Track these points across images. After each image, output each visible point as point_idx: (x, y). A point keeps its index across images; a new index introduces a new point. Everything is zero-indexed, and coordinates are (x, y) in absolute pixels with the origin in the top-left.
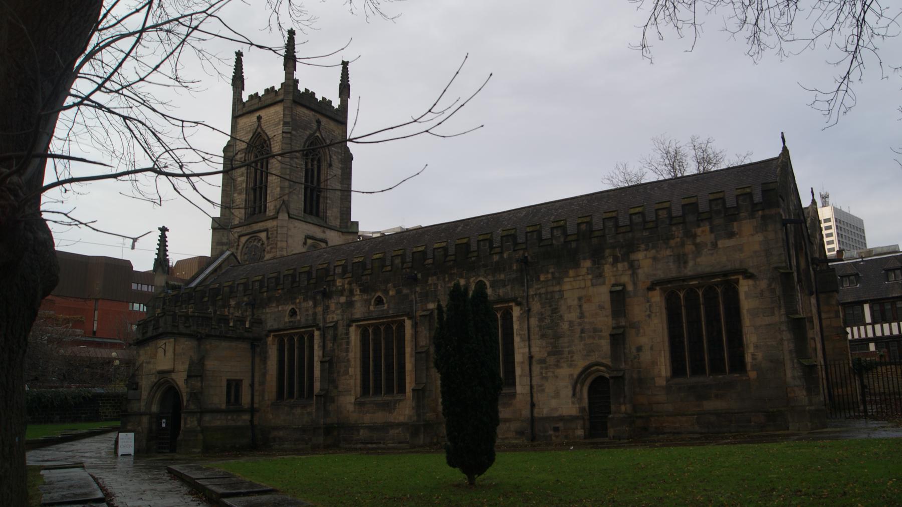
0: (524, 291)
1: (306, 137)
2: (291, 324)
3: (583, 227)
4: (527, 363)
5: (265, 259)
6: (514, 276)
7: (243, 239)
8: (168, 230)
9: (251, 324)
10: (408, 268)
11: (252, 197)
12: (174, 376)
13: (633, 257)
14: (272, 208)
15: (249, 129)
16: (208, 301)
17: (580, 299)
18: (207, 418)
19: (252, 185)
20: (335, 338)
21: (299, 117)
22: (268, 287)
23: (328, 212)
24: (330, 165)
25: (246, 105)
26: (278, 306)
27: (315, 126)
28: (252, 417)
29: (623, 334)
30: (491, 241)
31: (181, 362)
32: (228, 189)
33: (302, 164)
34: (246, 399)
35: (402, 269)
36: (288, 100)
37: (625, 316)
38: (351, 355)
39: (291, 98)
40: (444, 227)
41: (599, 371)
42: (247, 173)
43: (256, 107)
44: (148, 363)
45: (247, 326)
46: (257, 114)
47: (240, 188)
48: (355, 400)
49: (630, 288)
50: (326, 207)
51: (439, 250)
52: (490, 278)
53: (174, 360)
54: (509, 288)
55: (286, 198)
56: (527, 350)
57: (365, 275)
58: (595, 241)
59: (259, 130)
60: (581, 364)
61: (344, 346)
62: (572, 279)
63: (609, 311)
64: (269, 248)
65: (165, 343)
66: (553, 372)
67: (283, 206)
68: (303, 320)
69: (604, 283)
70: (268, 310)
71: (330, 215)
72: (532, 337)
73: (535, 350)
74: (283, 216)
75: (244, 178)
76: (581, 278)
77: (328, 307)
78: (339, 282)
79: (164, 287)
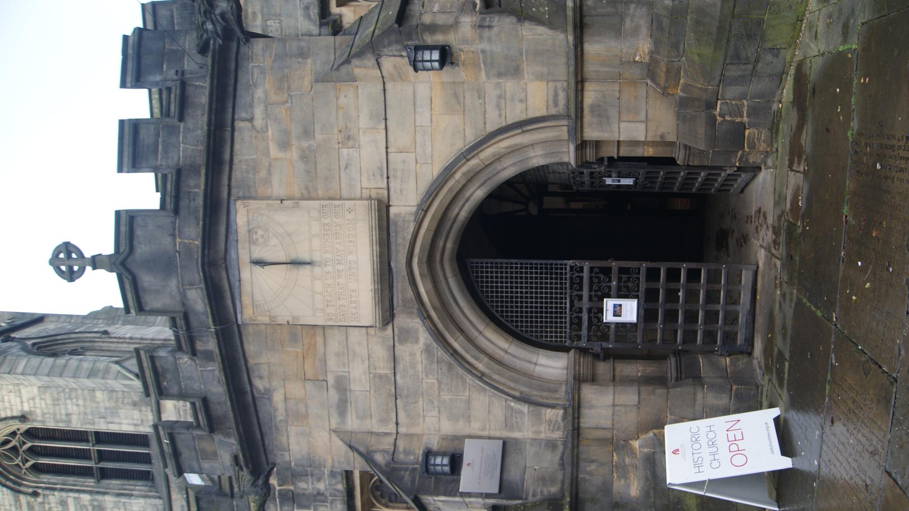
31: (345, 152)
42: (62, 490)
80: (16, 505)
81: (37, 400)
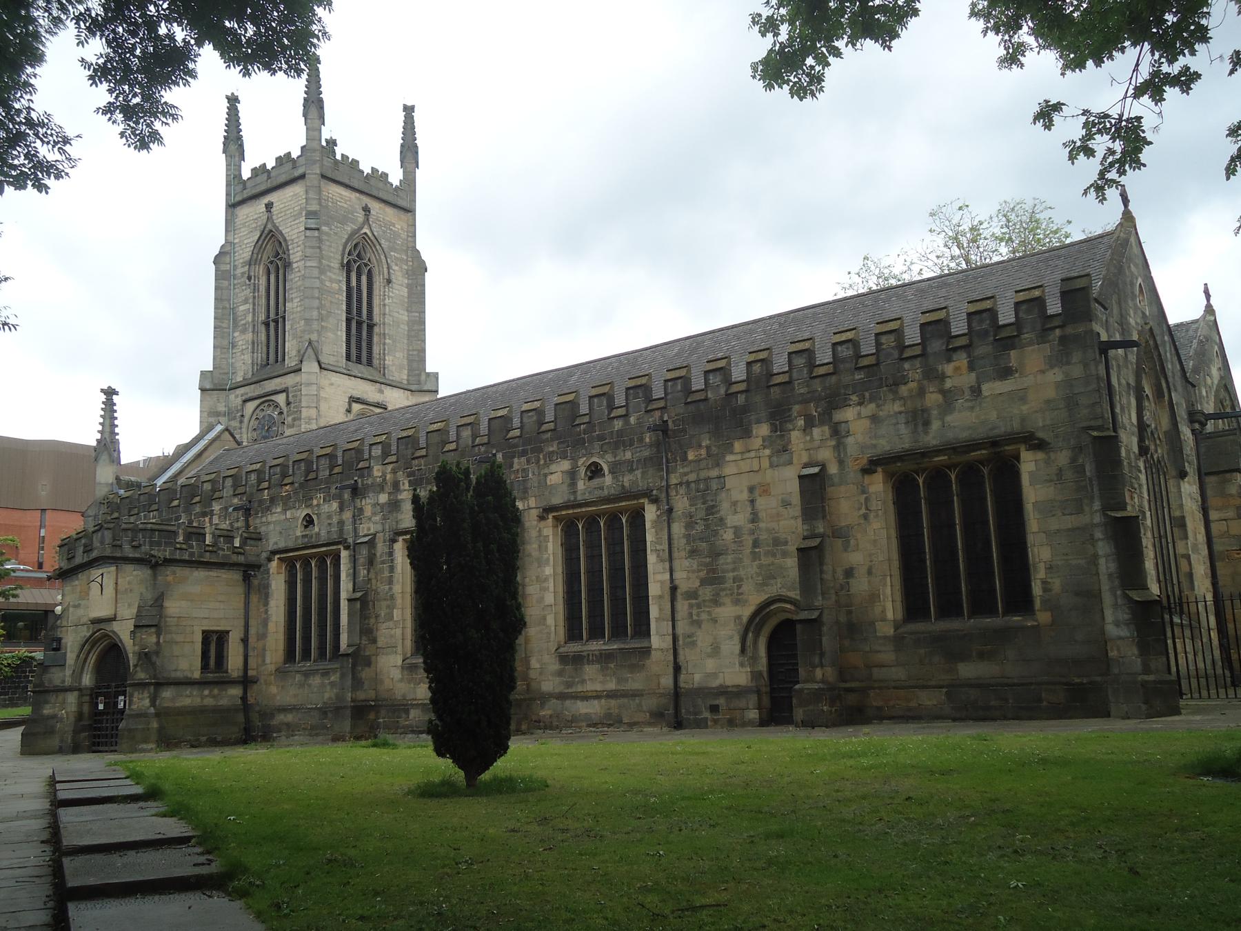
0: (662, 478)
1: (346, 237)
2: (306, 540)
3: (757, 368)
4: (667, 597)
5: (285, 435)
6: (647, 453)
7: (251, 406)
8: (117, 393)
9: (244, 541)
10: (482, 445)
11: (263, 337)
12: (116, 626)
13: (839, 416)
14: (294, 353)
15: (254, 225)
16: (179, 506)
17: (751, 489)
18: (167, 693)
19: (262, 317)
20: (371, 561)
21: (332, 203)
22: (269, 481)
23: (387, 358)
24: (389, 281)
25: (248, 185)
26: (285, 510)
27: (360, 216)
28: (245, 692)
29: (819, 549)
30: (609, 397)
32: (224, 325)
33: (340, 281)
34: (234, 662)
35: (473, 447)
36: (313, 174)
37: (824, 517)
38: (397, 588)
39: (318, 172)
40: (552, 374)
41: (785, 610)
42: (254, 297)
43: (263, 188)
44: (77, 606)
45: (237, 544)
46: (266, 200)
47: (243, 322)
48: (403, 661)
49: (833, 469)
50: (384, 350)
51: (530, 414)
52: (610, 458)
53: (116, 601)
54: (638, 473)
55: (314, 337)
56: (667, 576)
57: (417, 458)
58: (775, 393)
59: (270, 226)
60: (755, 599)
61: (387, 574)
62: (739, 457)
63: (796, 510)
64: (290, 419)
65: (102, 574)
66: (709, 613)
67: (310, 350)
68: (323, 533)
69: (790, 463)
70: (270, 518)
71: (390, 363)
72: (675, 555)
73: (680, 575)
74: (310, 367)
75: (249, 306)
76: (753, 454)
77: (361, 510)
78: (377, 471)
79: (112, 484)
80: (244, 263)
81: (299, 274)
